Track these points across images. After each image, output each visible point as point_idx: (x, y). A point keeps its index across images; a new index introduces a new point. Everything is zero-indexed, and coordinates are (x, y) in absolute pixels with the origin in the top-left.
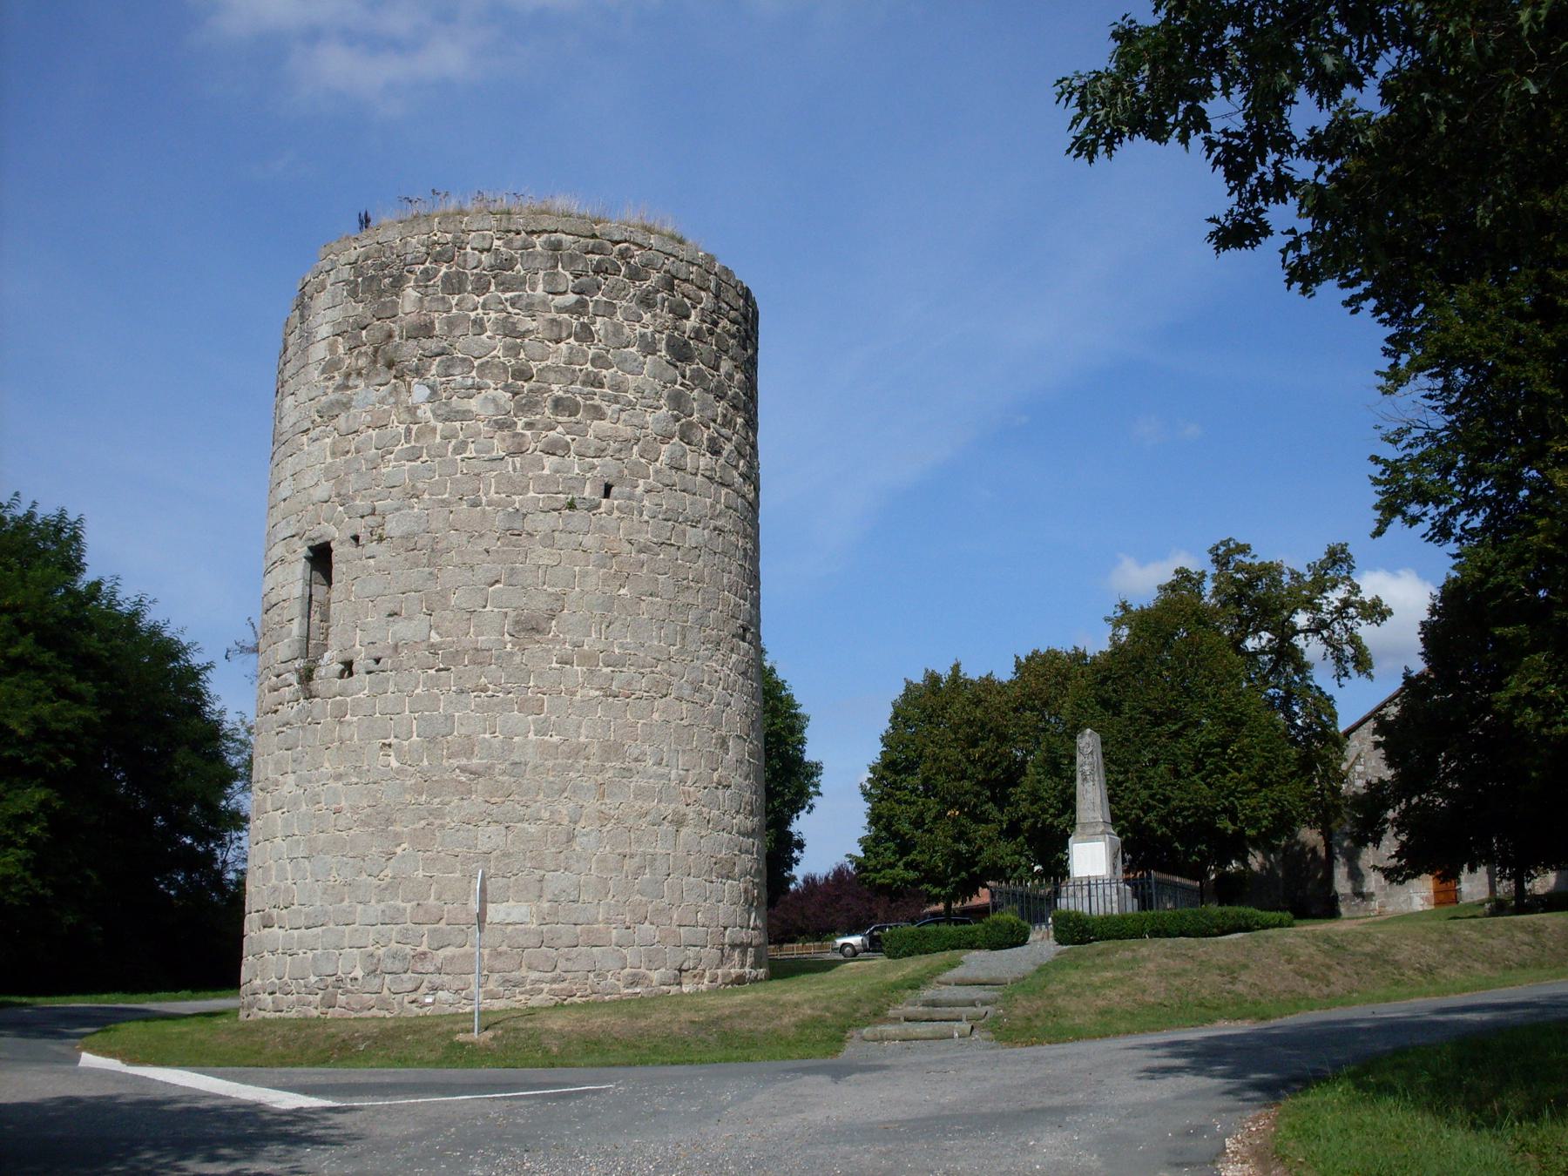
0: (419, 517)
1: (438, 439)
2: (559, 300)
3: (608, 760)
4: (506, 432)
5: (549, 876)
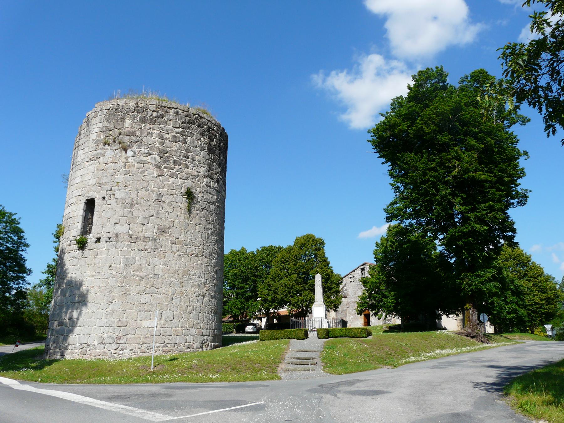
0: (127, 193)
1: (135, 169)
2: (177, 130)
3: (184, 275)
4: (158, 169)
5: (164, 312)
